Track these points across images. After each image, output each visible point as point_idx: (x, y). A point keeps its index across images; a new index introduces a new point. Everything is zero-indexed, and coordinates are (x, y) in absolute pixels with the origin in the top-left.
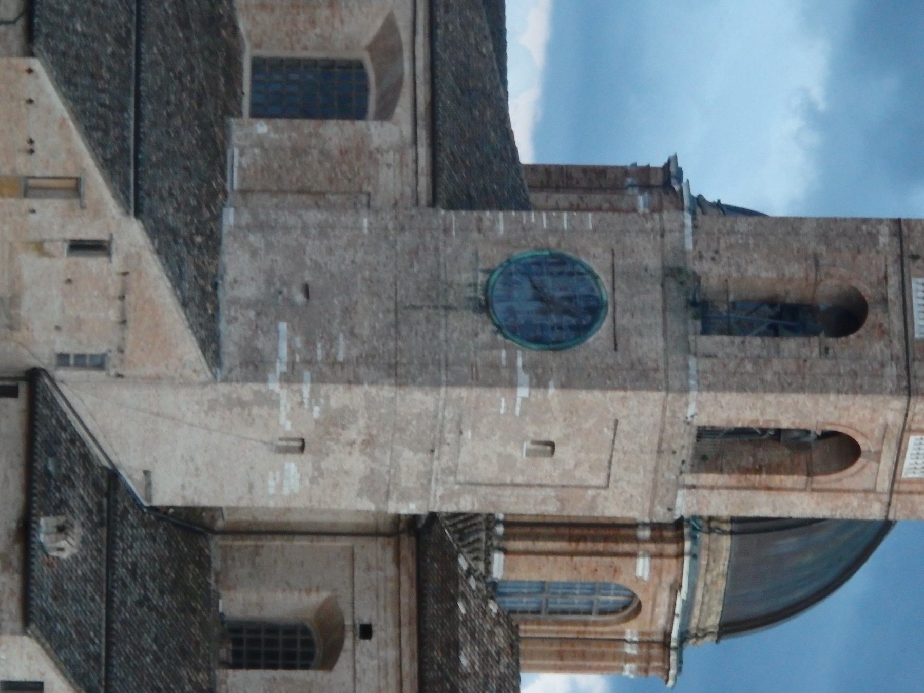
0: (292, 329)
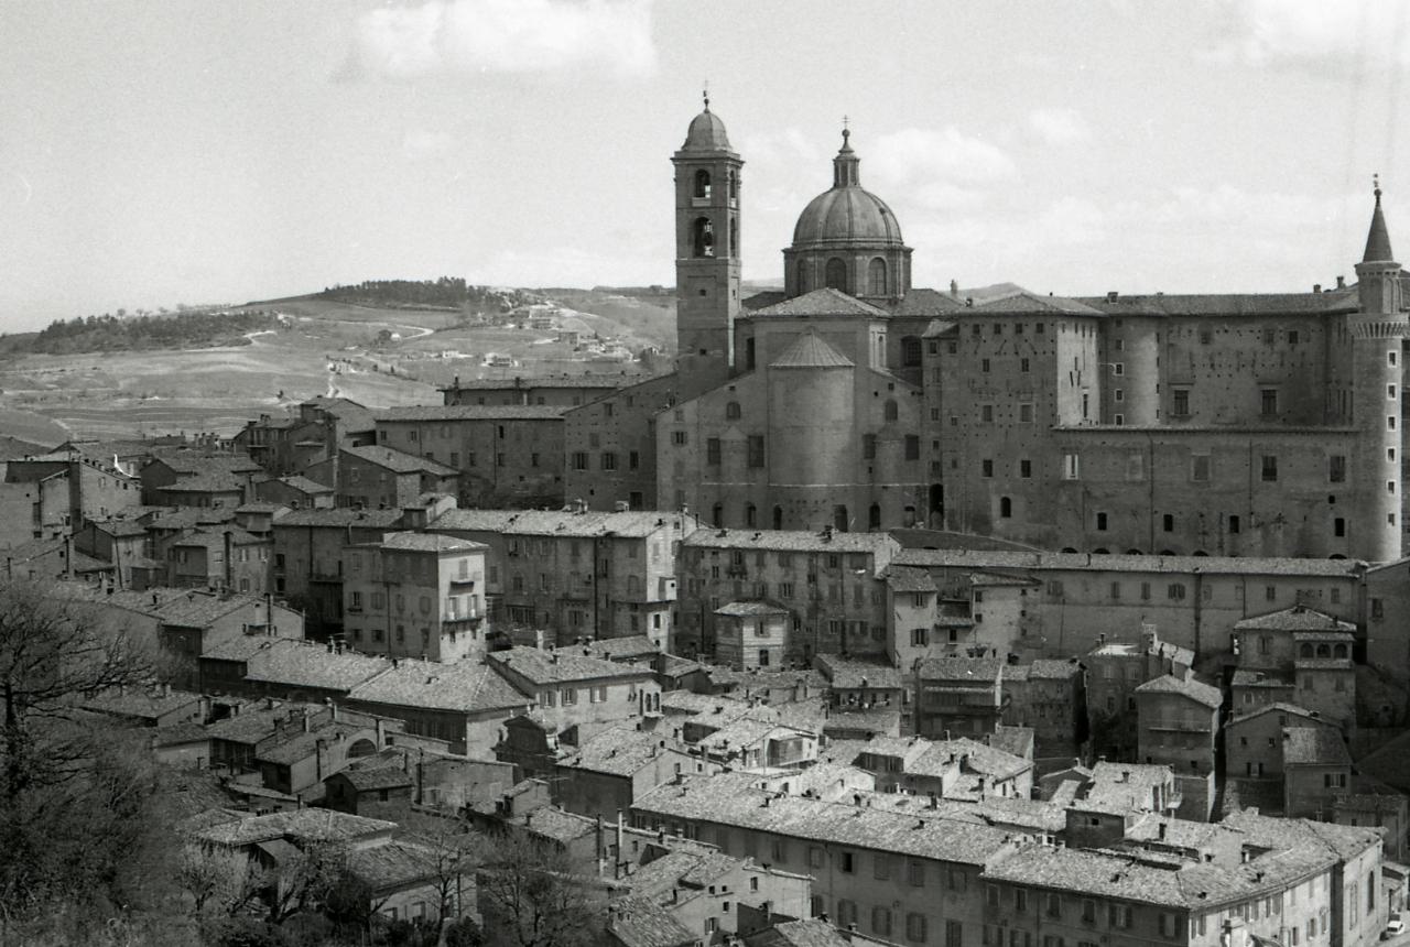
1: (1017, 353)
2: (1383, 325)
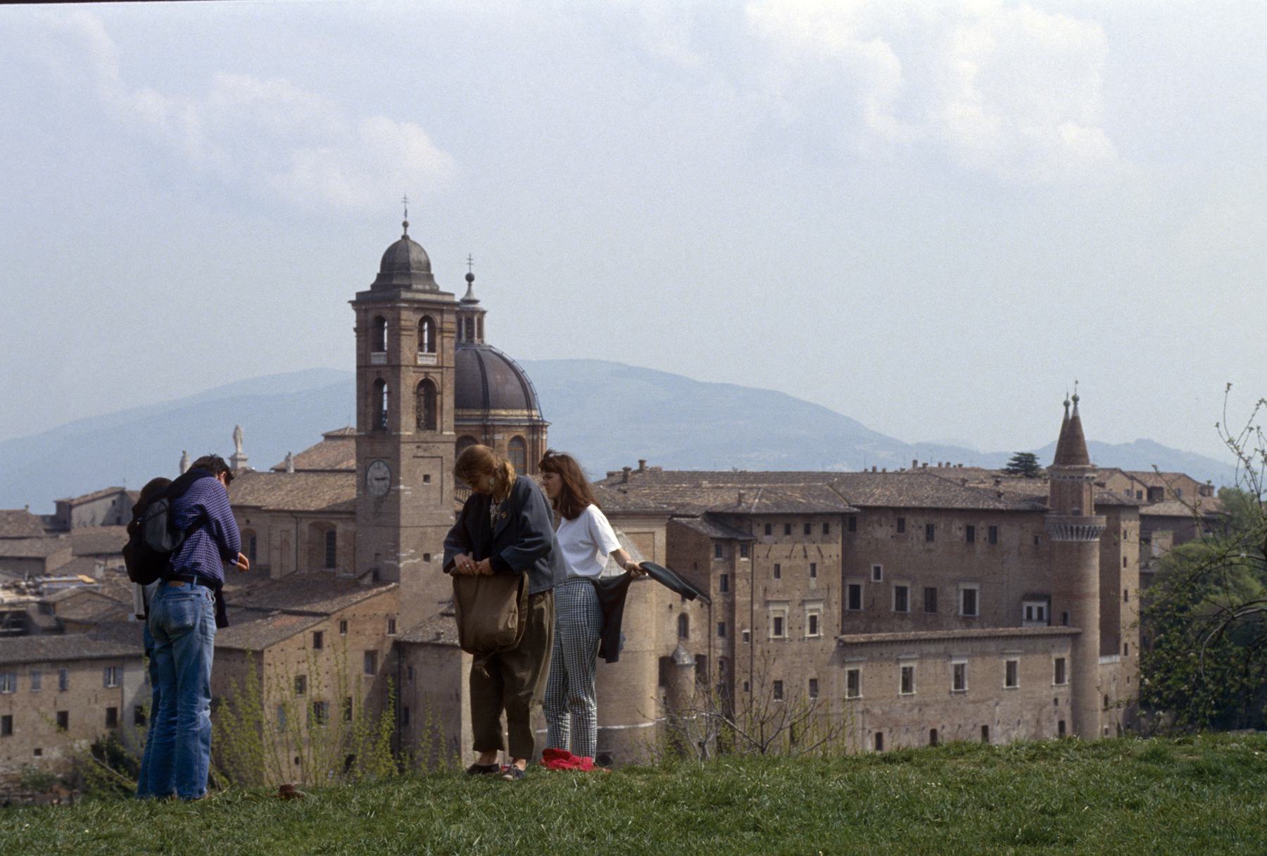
0: (387, 559)
1: (806, 556)
2: (1078, 528)
